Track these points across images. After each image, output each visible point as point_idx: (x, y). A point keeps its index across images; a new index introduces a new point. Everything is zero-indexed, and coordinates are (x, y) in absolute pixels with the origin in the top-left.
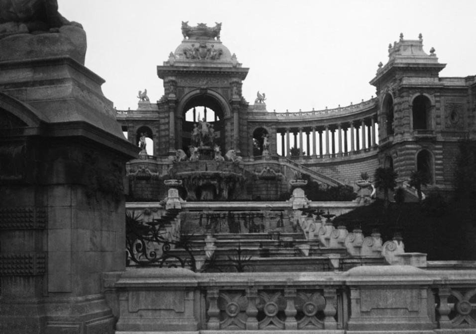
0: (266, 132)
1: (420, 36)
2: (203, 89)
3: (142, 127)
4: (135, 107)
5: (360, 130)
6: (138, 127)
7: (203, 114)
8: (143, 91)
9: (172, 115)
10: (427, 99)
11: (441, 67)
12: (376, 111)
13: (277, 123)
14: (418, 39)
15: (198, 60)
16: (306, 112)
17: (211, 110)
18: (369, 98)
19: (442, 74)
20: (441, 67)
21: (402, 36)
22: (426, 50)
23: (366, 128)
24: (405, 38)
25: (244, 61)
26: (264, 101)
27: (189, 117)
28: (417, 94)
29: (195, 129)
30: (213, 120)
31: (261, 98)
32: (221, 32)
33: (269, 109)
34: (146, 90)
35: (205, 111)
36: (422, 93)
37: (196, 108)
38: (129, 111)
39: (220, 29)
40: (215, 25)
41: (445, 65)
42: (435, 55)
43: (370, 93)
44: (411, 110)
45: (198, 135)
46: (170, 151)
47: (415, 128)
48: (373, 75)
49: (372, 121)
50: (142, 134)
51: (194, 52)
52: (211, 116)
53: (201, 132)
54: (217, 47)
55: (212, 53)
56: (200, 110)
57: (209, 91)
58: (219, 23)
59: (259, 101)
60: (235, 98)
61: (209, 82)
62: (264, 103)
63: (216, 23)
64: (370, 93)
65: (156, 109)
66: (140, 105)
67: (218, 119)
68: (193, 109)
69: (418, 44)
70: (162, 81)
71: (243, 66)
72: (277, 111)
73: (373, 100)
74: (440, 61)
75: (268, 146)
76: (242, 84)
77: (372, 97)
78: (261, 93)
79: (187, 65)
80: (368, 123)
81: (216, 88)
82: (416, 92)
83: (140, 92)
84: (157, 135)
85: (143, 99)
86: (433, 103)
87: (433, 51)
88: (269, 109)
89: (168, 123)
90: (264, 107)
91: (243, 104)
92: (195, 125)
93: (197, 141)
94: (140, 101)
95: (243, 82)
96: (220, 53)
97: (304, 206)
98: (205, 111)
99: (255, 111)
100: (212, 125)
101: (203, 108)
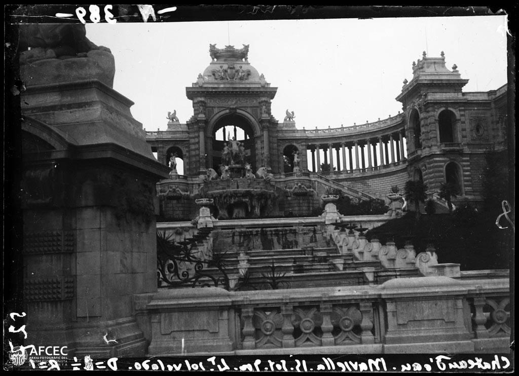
0: (296, 149)
1: (443, 54)
2: (233, 109)
3: (172, 148)
5: (389, 145)
6: (167, 148)
7: (233, 134)
8: (172, 112)
9: (202, 134)
11: (464, 82)
12: (404, 126)
13: (307, 140)
14: (441, 57)
15: (226, 81)
16: (335, 129)
17: (241, 129)
18: (397, 114)
19: (465, 89)
20: (464, 82)
21: (424, 54)
22: (449, 67)
23: (395, 142)
24: (427, 56)
25: (272, 81)
26: (293, 119)
27: (219, 136)
28: (443, 109)
29: (226, 148)
30: (243, 138)
31: (290, 116)
32: (249, 55)
33: (299, 127)
34: (175, 111)
35: (235, 130)
36: (447, 108)
37: (226, 127)
38: (159, 132)
39: (247, 51)
40: (242, 47)
41: (468, 80)
42: (457, 71)
43: (397, 108)
44: (437, 124)
45: (228, 153)
46: (201, 171)
47: (441, 142)
48: (399, 92)
49: (400, 135)
50: (172, 154)
51: (223, 74)
52: (241, 135)
53: (231, 151)
54: (245, 67)
55: (240, 74)
56: (230, 129)
58: (247, 45)
59: (288, 119)
61: (239, 102)
62: (294, 121)
63: (244, 45)
64: (397, 108)
65: (186, 129)
66: (169, 125)
67: (248, 138)
68: (223, 128)
69: (441, 61)
70: (191, 102)
71: (271, 86)
72: (306, 129)
73: (400, 115)
74: (463, 77)
75: (298, 163)
76: (271, 103)
77: (399, 112)
78: (290, 112)
79: (216, 86)
80: (396, 138)
81: (245, 107)
82: (441, 107)
84: (187, 154)
85: (173, 120)
86: (458, 117)
87: (455, 67)
88: (299, 127)
89: (198, 143)
90: (293, 124)
91: (272, 123)
92: (225, 144)
93: (227, 159)
94: (169, 122)
95: (271, 101)
96: (249, 74)
97: (336, 221)
98: (235, 130)
99: (285, 129)
100: (243, 144)
101: (233, 127)
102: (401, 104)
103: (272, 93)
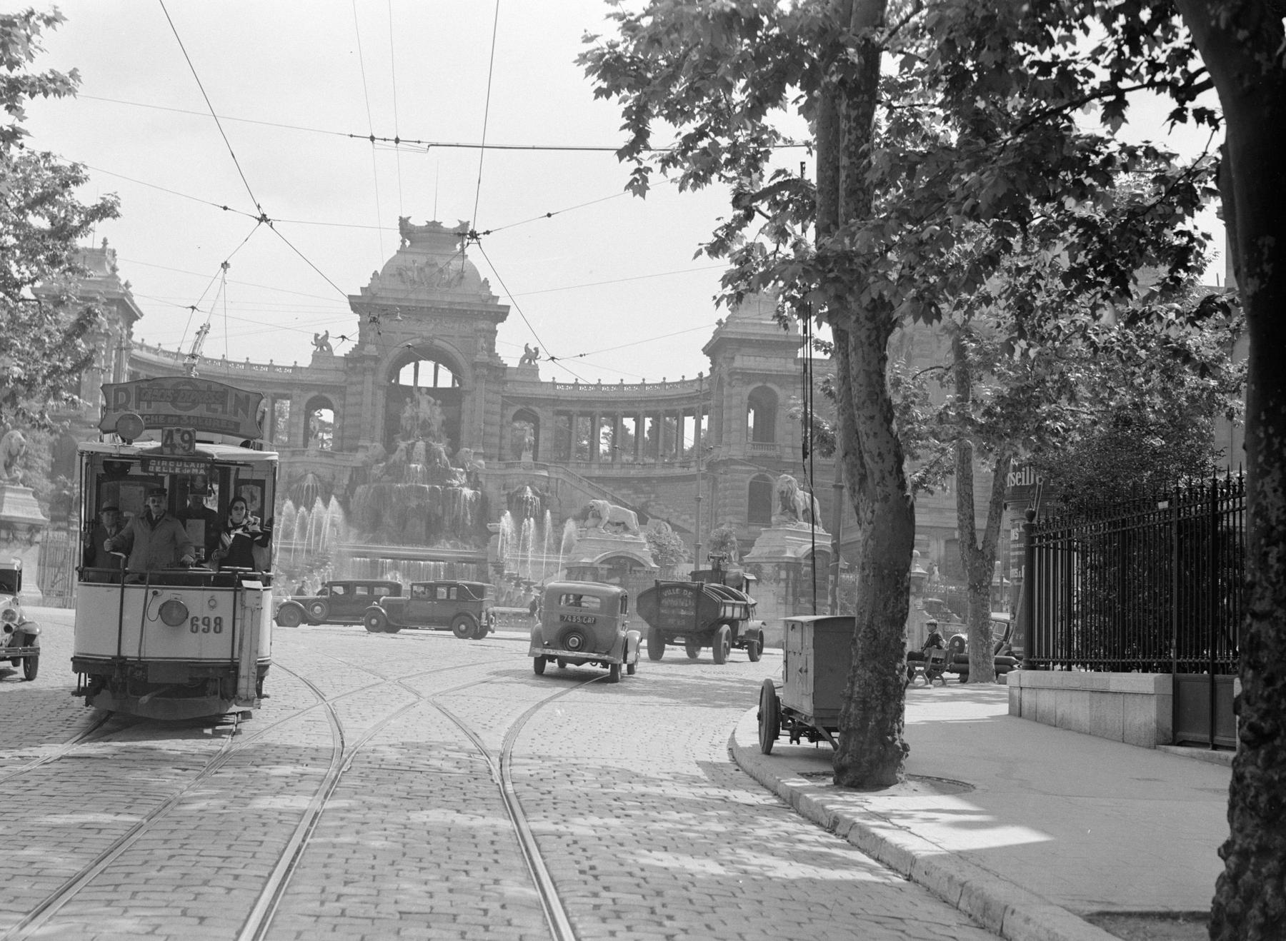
3: (314, 398)
4: (305, 361)
8: (322, 334)
10: (771, 392)
27: (406, 376)
30: (450, 385)
37: (421, 363)
45: (412, 418)
56: (426, 366)
57: (437, 342)
60: (482, 357)
66: (315, 355)
68: (413, 364)
76: (496, 332)
78: (531, 347)
79: (401, 296)
83: (317, 335)
89: (361, 393)
91: (497, 370)
96: (461, 275)
99: (518, 378)
102: (708, 360)
103: (501, 314)
